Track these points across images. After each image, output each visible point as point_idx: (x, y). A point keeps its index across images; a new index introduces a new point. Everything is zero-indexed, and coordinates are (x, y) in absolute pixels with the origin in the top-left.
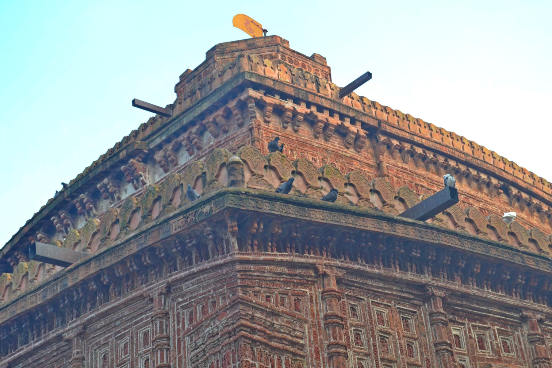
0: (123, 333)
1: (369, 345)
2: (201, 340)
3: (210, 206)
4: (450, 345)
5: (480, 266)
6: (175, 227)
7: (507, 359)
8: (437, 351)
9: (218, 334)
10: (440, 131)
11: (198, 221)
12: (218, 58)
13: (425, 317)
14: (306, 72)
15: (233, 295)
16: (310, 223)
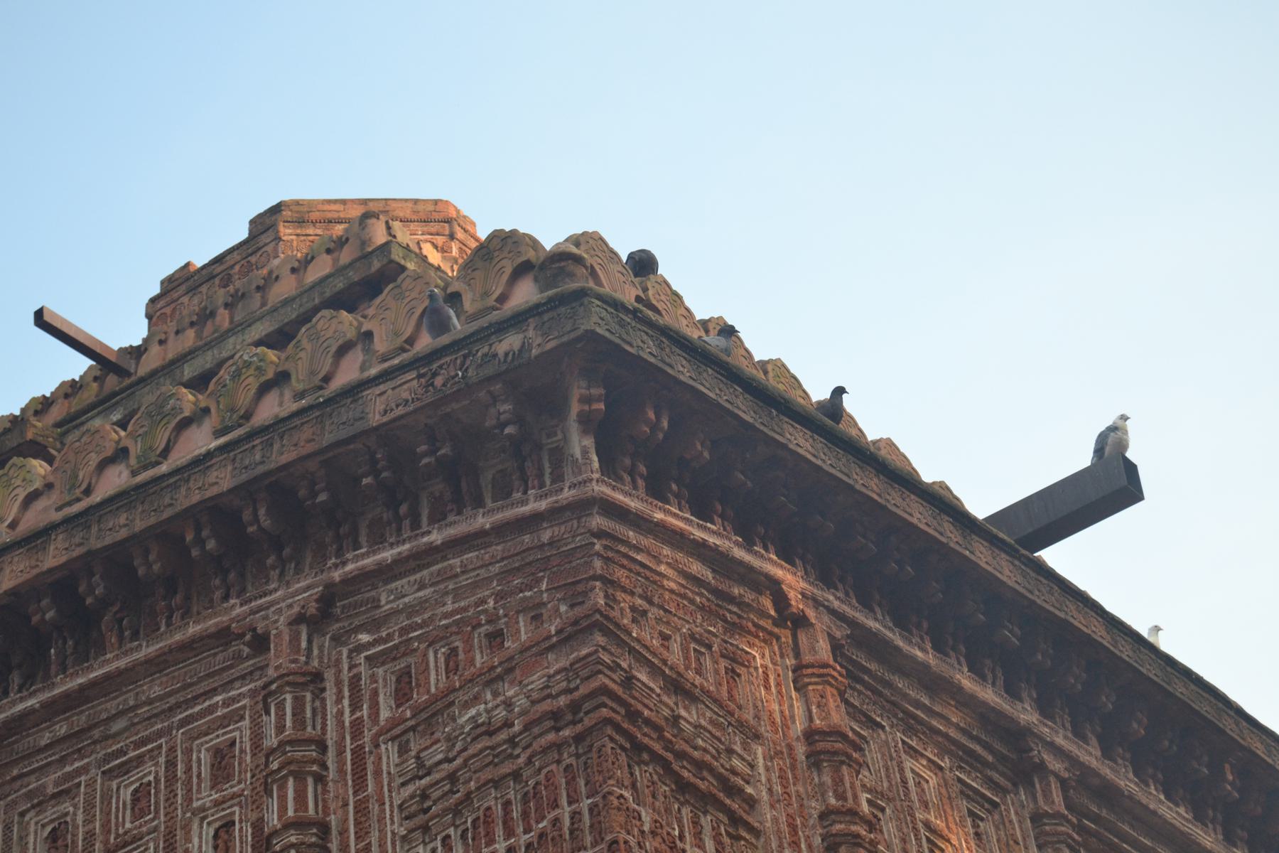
0: (132, 754)
2: (441, 746)
3: (521, 336)
9: (508, 724)
15: (572, 606)
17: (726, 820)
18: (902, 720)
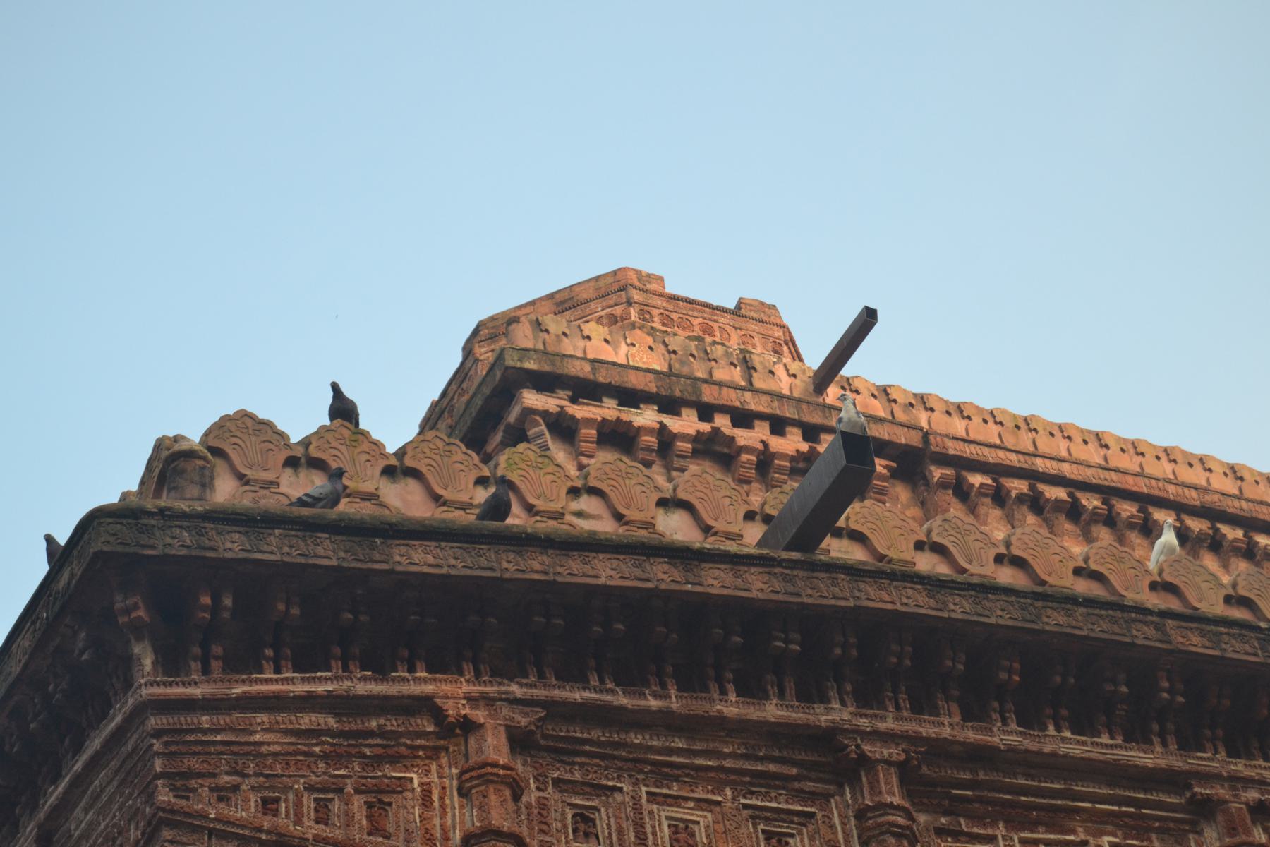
5: (1016, 666)
12: (484, 350)
13: (843, 824)
14: (715, 343)
18: (651, 772)
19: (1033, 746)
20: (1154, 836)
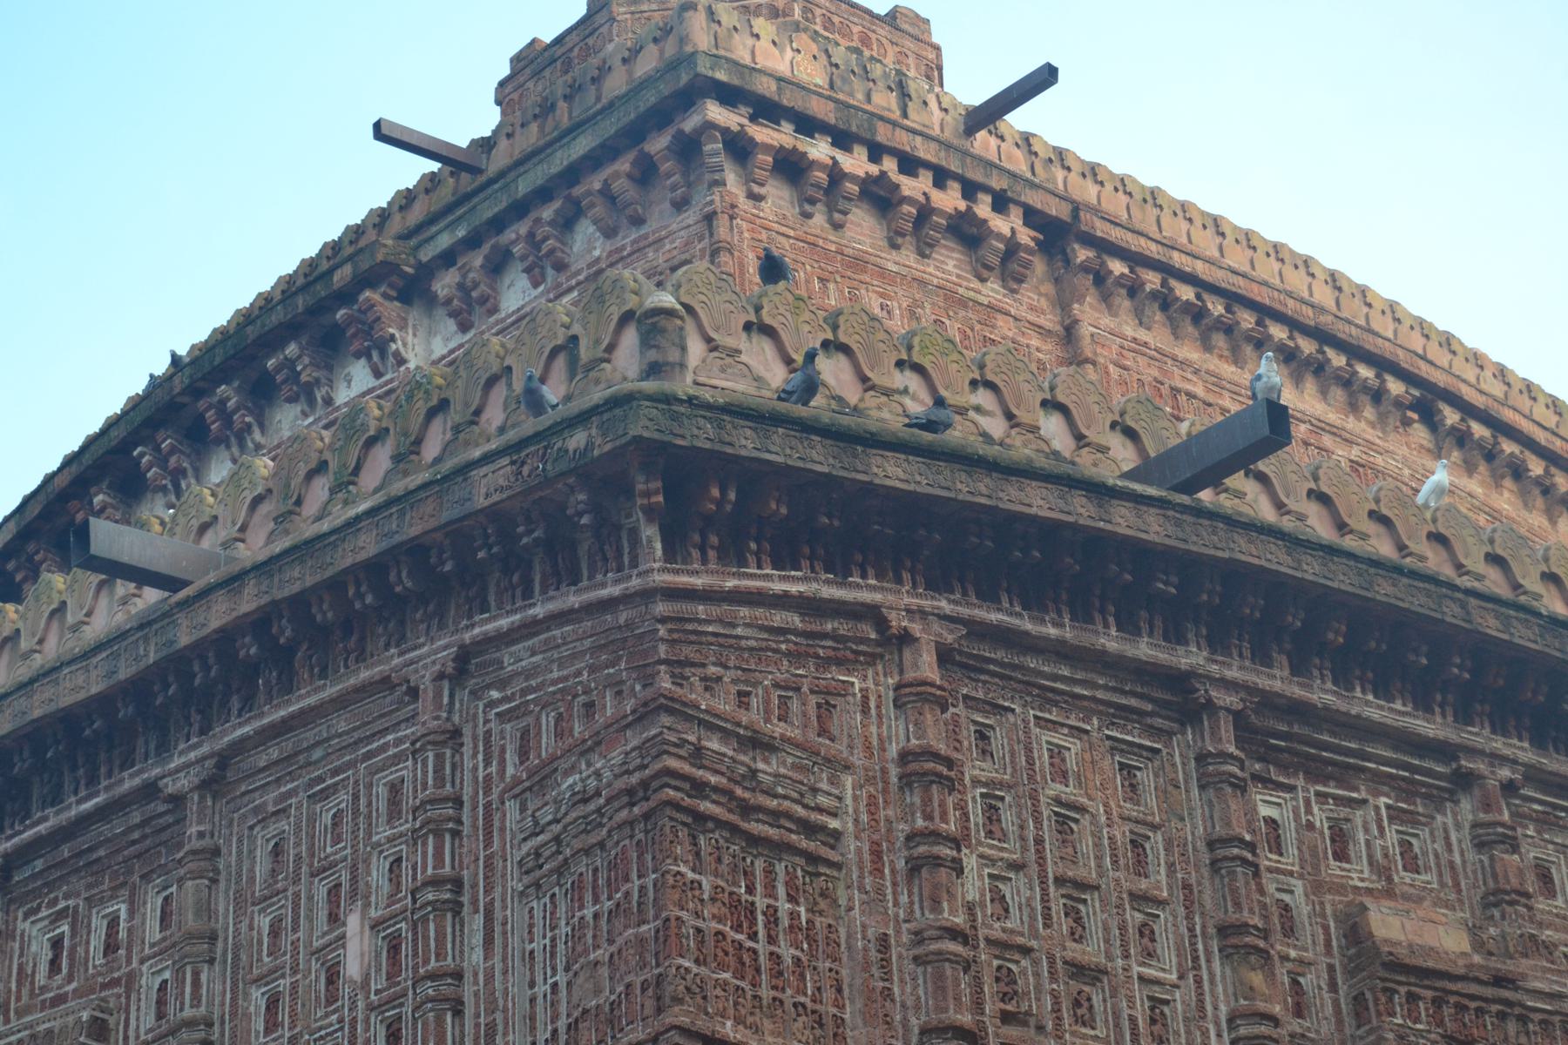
0: (329, 782)
1: (1023, 839)
2: (550, 808)
4: (1252, 847)
5: (1344, 628)
6: (488, 488)
7: (1412, 891)
8: (1213, 863)
9: (598, 794)
10: (1248, 239)
11: (551, 474)
12: (622, 10)
13: (1184, 764)
14: (872, 58)
15: (644, 686)
16: (869, 489)
17: (802, 862)
19: (1342, 706)
20: (1419, 801)
